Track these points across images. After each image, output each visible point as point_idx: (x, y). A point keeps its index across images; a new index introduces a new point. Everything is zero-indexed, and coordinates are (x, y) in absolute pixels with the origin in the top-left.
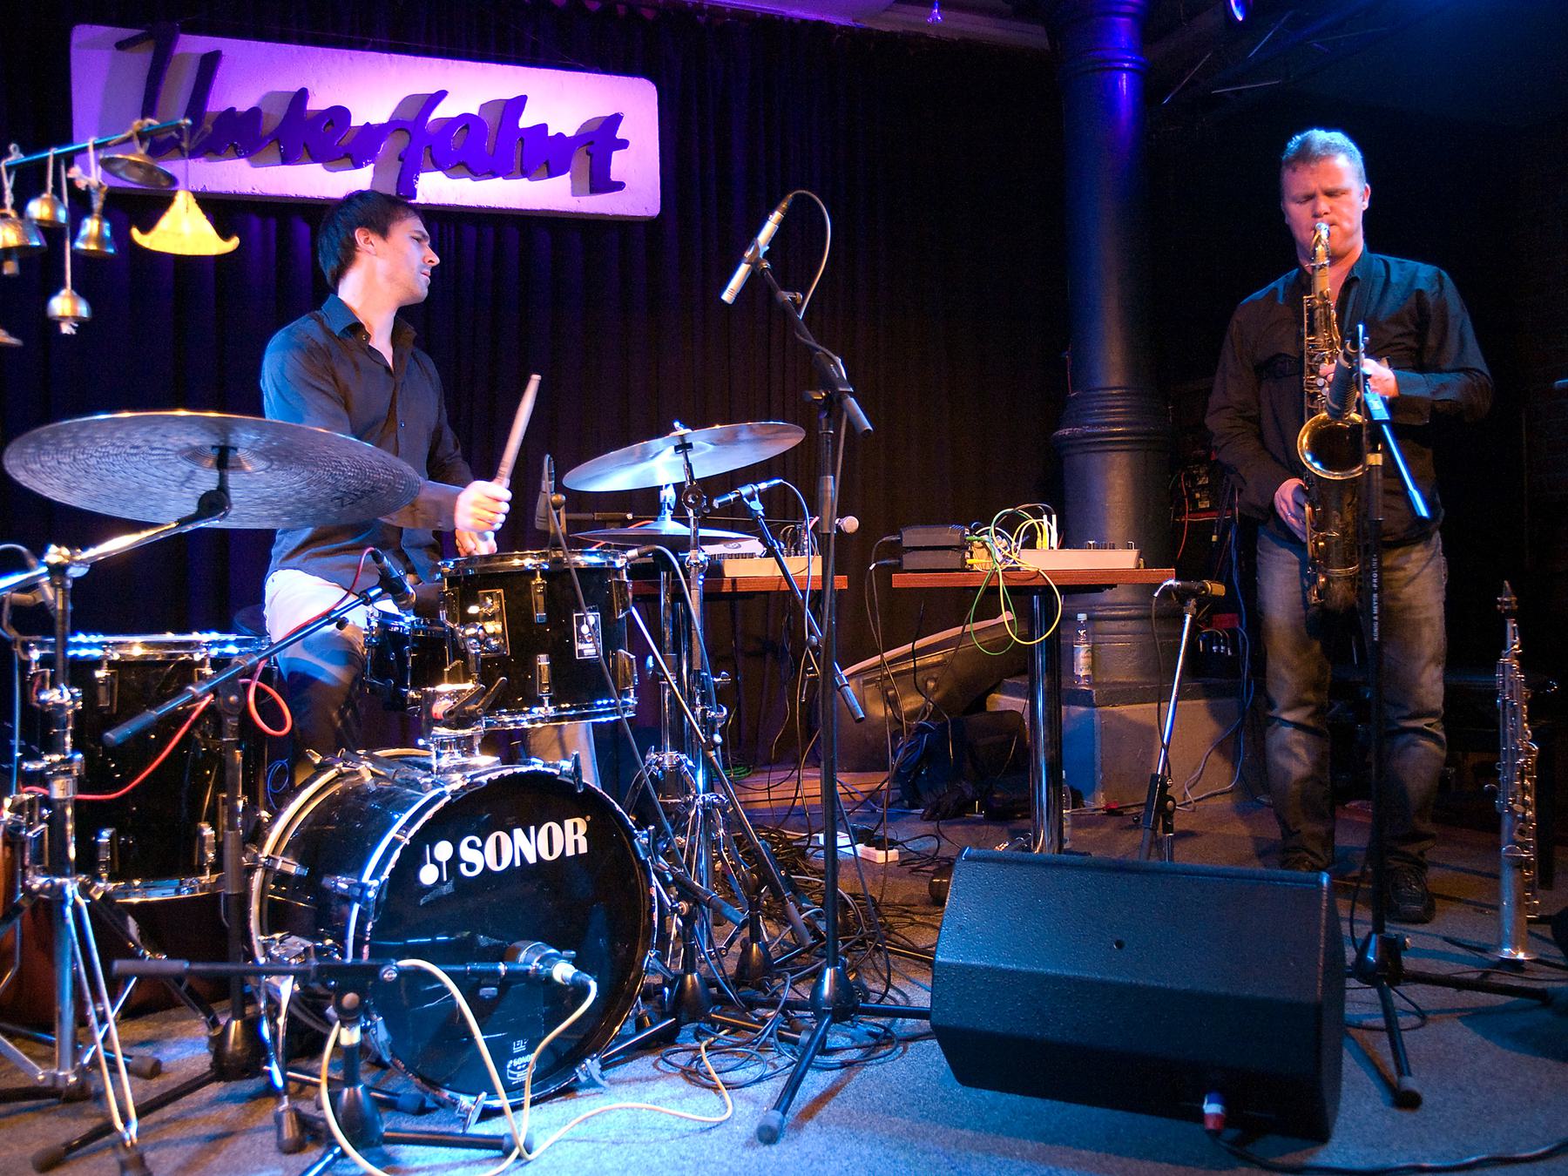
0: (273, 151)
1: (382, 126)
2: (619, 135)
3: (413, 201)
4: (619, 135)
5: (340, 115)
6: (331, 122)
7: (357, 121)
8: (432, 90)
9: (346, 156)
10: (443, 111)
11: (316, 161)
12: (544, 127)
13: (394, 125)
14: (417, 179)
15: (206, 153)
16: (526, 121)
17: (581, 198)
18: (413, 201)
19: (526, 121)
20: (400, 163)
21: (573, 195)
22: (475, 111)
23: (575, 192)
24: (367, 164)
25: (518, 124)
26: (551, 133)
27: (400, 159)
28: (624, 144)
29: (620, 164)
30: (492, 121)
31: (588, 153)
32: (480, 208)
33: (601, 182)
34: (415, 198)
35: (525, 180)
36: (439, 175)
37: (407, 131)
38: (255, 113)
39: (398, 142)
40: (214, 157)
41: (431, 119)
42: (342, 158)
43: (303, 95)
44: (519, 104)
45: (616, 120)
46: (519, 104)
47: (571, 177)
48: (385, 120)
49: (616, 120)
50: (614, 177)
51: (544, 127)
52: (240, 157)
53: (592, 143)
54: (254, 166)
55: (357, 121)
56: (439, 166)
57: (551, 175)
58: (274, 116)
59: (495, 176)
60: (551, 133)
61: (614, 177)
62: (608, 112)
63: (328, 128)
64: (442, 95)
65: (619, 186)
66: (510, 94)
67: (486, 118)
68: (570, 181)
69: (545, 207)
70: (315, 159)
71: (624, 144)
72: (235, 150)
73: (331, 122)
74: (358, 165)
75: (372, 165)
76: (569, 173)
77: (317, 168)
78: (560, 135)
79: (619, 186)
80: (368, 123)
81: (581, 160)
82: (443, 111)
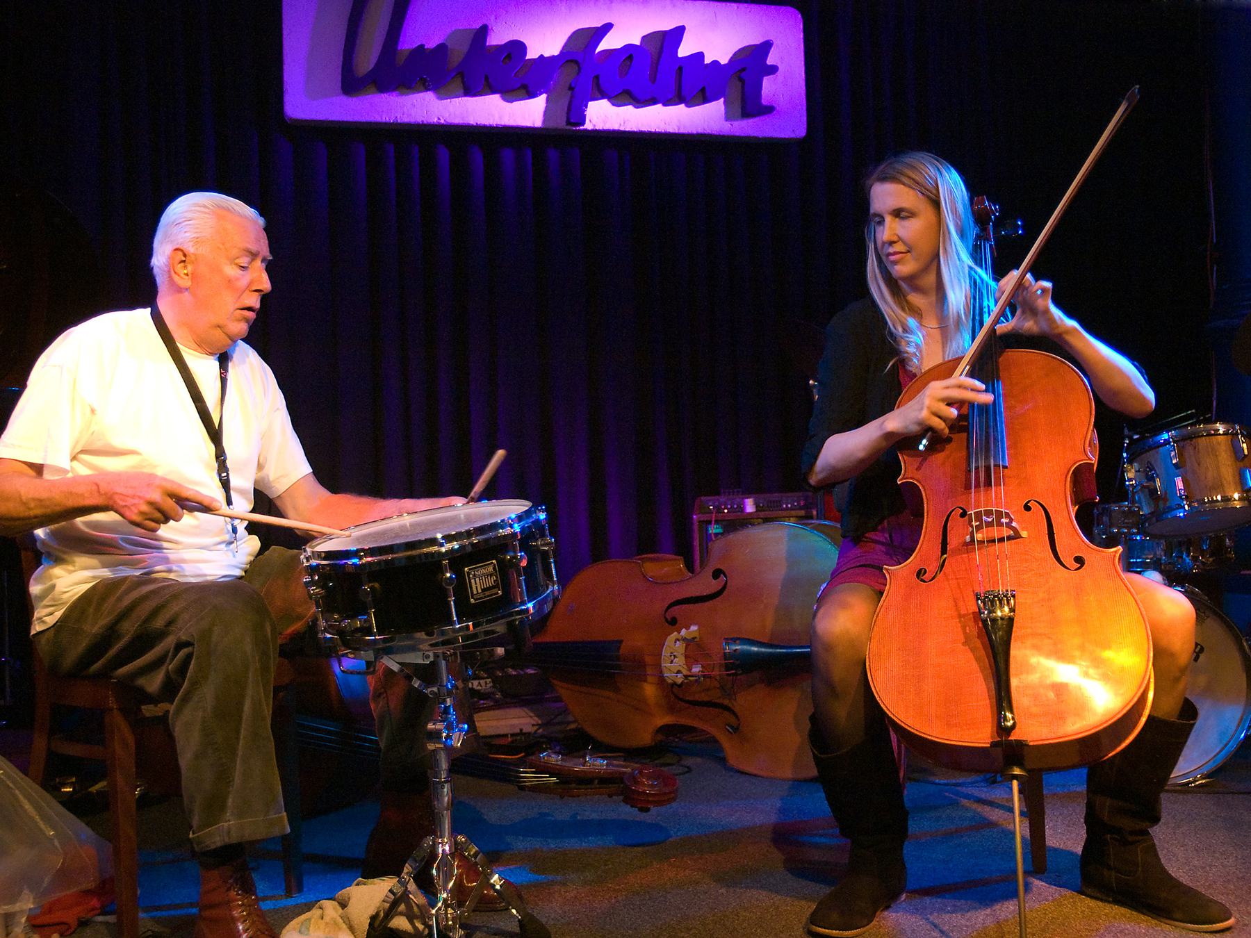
0: (457, 84)
1: (553, 57)
3: (582, 128)
5: (518, 48)
7: (532, 54)
9: (524, 87)
11: (494, 93)
12: (700, 56)
14: (587, 107)
15: (397, 88)
16: (684, 51)
17: (736, 124)
18: (582, 128)
19: (684, 51)
20: (570, 92)
21: (726, 121)
22: (638, 43)
23: (728, 117)
25: (677, 52)
26: (707, 61)
27: (571, 88)
30: (653, 49)
31: (741, 79)
32: (641, 133)
33: (751, 105)
34: (583, 123)
35: (682, 106)
36: (604, 103)
37: (576, 62)
38: (442, 48)
39: (568, 74)
40: (405, 91)
41: (599, 49)
42: (519, 88)
43: (484, 31)
44: (678, 33)
45: (766, 46)
46: (678, 33)
47: (724, 102)
48: (556, 53)
49: (766, 46)
50: (764, 102)
51: (700, 56)
52: (427, 90)
53: (744, 69)
54: (440, 98)
55: (532, 54)
57: (706, 100)
58: (458, 52)
59: (655, 103)
60: (707, 61)
62: (757, 40)
64: (608, 27)
66: (667, 25)
68: (723, 107)
69: (700, 130)
71: (773, 70)
72: (424, 85)
73: (509, 56)
74: (532, 95)
75: (544, 96)
76: (722, 100)
77: (496, 98)
78: (715, 63)
79: (769, 110)
80: (542, 56)
81: (734, 88)
82: (609, 43)
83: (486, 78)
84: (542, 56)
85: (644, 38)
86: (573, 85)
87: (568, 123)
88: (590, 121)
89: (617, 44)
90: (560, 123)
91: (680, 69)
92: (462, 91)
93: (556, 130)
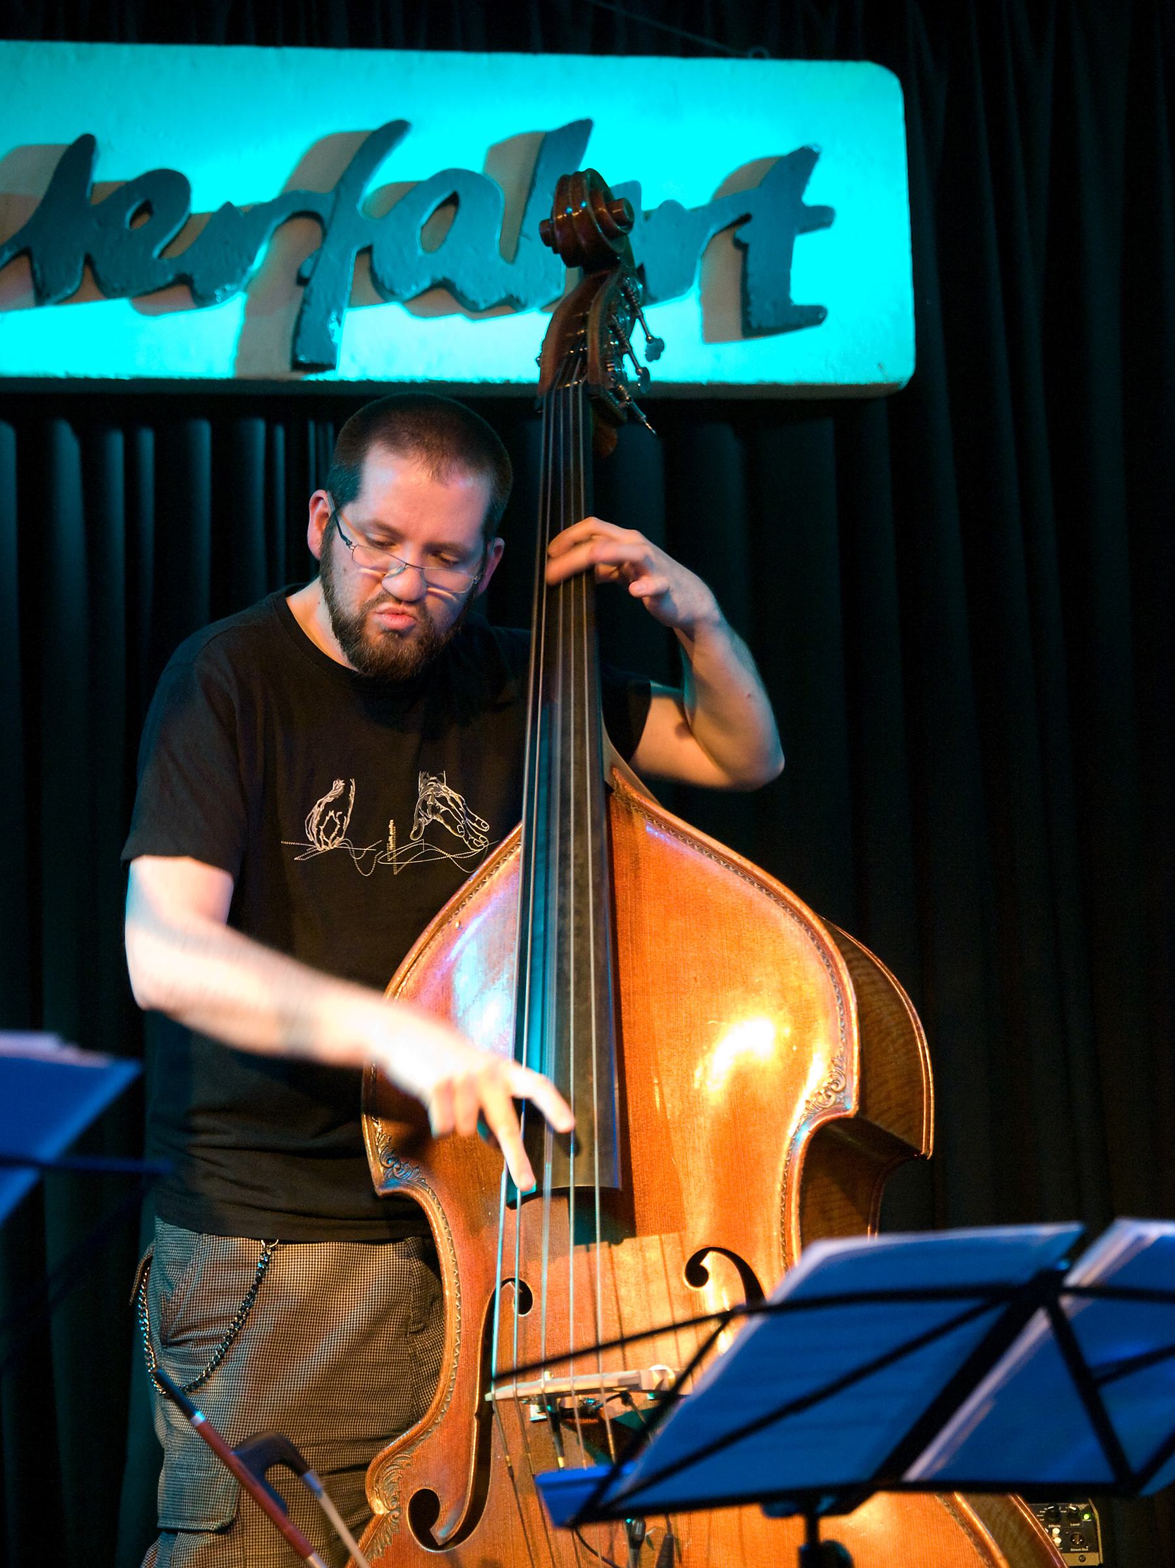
2: (812, 196)
4: (812, 196)
6: (145, 208)
8: (373, 123)
9: (184, 280)
20: (301, 290)
24: (226, 295)
27: (302, 281)
28: (821, 217)
42: (169, 286)
50: (801, 295)
53: (745, 219)
61: (801, 295)
62: (783, 146)
63: (144, 219)
64: (395, 131)
65: (813, 316)
70: (107, 290)
71: (821, 217)
73: (145, 208)
74: (202, 299)
78: (670, 207)
79: (813, 316)
83: (89, 261)
84: (228, 207)
86: (306, 274)
87: (297, 366)
88: (353, 358)
89: (422, 172)
92: (30, 295)
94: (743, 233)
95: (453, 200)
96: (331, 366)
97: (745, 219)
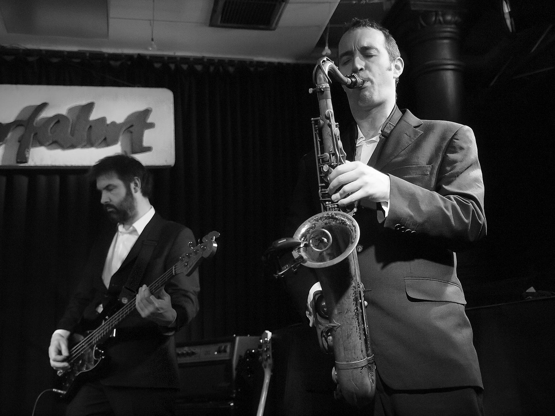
2: (150, 120)
4: (150, 120)
8: (39, 103)
10: (47, 114)
12: (103, 120)
13: (17, 124)
16: (94, 116)
19: (94, 116)
26: (109, 122)
27: (19, 141)
28: (152, 125)
29: (148, 138)
39: (19, 132)
44: (90, 107)
45: (147, 112)
46: (90, 107)
49: (147, 112)
50: (145, 144)
51: (103, 120)
53: (132, 126)
56: (41, 144)
60: (109, 122)
61: (145, 144)
65: (149, 149)
66: (84, 102)
67: (69, 117)
78: (113, 123)
79: (149, 149)
82: (47, 114)
85: (71, 110)
90: (12, 162)
91: (90, 127)
93: (10, 166)
94: (131, 129)
95: (58, 122)
96: (26, 162)
97: (132, 126)
